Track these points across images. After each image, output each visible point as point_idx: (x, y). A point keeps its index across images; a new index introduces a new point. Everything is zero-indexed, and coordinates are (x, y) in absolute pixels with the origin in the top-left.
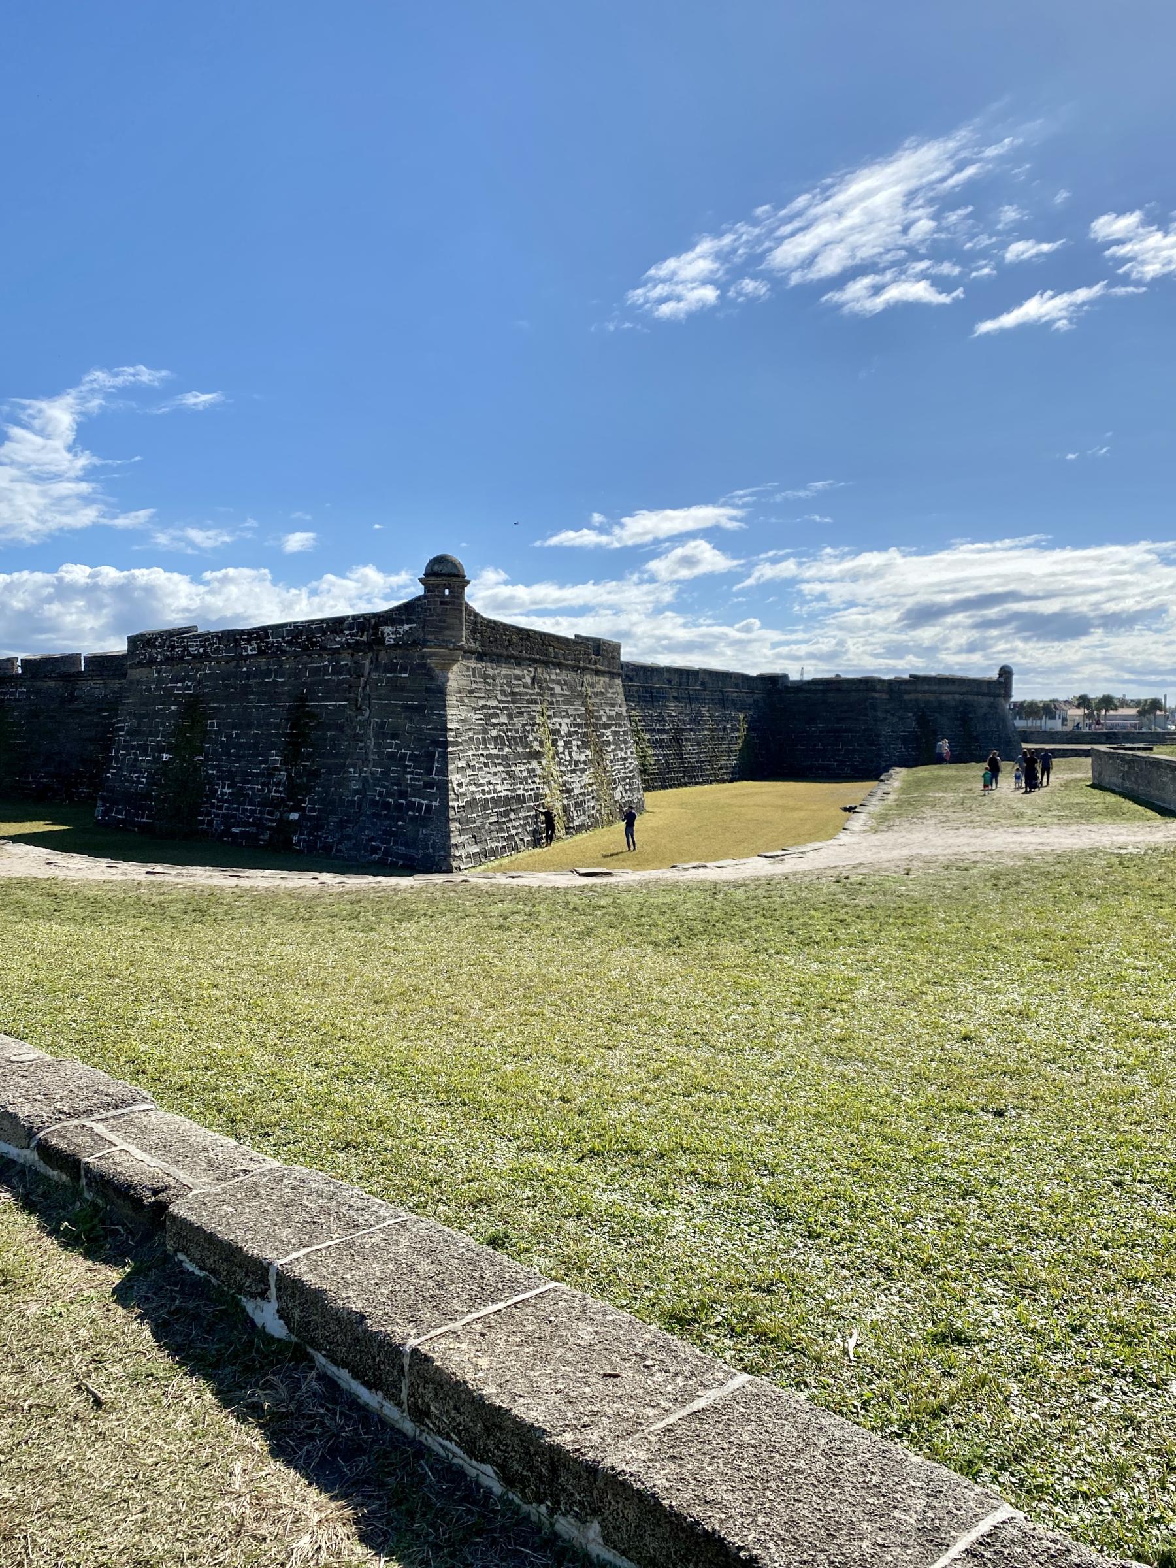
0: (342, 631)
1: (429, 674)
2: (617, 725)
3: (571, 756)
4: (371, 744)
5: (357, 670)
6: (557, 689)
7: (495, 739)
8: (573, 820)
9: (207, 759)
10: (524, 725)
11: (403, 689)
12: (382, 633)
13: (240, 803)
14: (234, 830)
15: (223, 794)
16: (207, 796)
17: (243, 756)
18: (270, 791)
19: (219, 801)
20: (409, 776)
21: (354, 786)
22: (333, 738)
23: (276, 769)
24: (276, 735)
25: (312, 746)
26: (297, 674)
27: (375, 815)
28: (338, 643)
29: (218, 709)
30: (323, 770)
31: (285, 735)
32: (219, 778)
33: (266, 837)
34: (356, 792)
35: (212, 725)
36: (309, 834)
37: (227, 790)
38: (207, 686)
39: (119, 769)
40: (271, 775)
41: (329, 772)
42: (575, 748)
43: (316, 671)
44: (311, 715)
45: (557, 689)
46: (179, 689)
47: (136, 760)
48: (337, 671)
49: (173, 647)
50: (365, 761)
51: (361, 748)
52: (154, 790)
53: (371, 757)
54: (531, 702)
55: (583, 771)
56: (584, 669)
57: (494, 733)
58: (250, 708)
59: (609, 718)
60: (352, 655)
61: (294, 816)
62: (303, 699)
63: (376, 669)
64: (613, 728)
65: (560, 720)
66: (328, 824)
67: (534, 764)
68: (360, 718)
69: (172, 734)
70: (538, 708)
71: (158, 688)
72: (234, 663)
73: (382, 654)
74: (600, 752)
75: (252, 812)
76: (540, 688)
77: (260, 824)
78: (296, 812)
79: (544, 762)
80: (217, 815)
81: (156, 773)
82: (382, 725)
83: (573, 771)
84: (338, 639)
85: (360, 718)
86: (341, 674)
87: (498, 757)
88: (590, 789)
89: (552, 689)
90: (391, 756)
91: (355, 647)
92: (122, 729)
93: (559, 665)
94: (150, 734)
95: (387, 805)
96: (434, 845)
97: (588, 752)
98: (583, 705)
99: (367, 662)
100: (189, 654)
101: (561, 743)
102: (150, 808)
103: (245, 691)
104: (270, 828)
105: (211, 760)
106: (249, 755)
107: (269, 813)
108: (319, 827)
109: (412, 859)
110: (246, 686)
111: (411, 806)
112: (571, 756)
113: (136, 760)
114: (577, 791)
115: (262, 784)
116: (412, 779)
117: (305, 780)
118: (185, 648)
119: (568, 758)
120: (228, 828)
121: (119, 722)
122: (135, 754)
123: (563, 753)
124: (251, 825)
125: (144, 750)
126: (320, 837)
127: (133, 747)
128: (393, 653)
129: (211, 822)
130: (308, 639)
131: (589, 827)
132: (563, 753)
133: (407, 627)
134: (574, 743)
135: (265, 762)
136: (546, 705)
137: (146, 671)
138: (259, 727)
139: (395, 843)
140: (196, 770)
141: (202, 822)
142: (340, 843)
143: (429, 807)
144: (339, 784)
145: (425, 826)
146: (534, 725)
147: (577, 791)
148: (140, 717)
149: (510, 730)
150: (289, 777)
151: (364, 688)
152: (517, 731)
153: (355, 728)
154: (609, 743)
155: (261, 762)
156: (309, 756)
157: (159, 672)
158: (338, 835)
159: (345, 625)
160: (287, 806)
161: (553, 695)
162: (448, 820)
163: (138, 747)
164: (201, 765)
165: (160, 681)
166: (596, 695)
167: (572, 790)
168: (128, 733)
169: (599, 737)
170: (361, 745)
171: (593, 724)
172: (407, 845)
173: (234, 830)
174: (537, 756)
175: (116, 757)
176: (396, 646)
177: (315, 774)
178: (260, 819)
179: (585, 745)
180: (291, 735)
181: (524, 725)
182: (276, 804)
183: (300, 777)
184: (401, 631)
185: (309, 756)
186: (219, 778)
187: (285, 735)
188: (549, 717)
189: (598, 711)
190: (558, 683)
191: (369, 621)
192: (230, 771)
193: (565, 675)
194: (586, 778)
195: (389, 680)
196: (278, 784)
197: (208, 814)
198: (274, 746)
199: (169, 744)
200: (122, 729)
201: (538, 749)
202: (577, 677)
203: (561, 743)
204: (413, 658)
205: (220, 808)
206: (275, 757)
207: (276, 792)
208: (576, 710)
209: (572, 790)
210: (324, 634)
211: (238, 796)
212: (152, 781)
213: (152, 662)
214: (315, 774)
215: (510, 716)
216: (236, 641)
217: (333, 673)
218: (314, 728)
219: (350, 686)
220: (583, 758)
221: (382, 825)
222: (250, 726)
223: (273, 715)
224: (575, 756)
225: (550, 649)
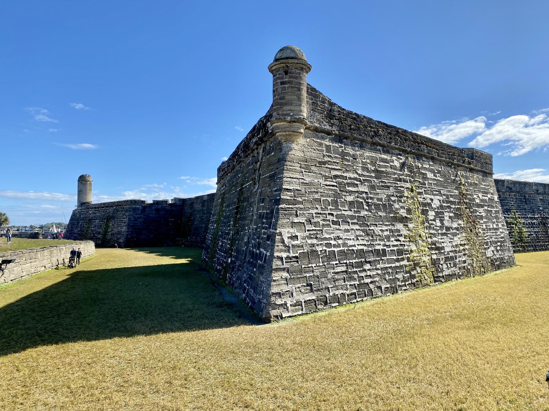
2: (488, 206)
3: (442, 221)
6: (430, 175)
7: (351, 203)
8: (442, 271)
10: (389, 196)
42: (447, 218)
45: (430, 175)
54: (400, 180)
55: (455, 235)
56: (459, 166)
57: (350, 198)
59: (482, 200)
64: (486, 208)
65: (432, 197)
67: (400, 226)
70: (408, 185)
74: (473, 221)
76: (410, 171)
79: (411, 226)
83: (443, 234)
87: (352, 217)
88: (462, 248)
89: (424, 174)
93: (433, 159)
97: (460, 222)
98: (457, 188)
101: (431, 214)
112: (443, 224)
114: (447, 249)
119: (439, 224)
123: (434, 220)
131: (461, 276)
132: (434, 220)
134: (446, 214)
136: (417, 184)
146: (401, 197)
147: (447, 249)
149: (371, 198)
152: (381, 200)
154: (481, 217)
161: (424, 177)
166: (470, 184)
167: (443, 248)
169: (471, 212)
171: (466, 203)
174: (404, 220)
179: (458, 216)
181: (389, 196)
188: (420, 193)
189: (472, 195)
190: (432, 171)
193: (436, 167)
194: (457, 240)
201: (405, 215)
202: (451, 171)
203: (431, 214)
208: (449, 191)
209: (443, 248)
215: (373, 187)
220: (455, 225)
224: (446, 224)
225: (423, 147)
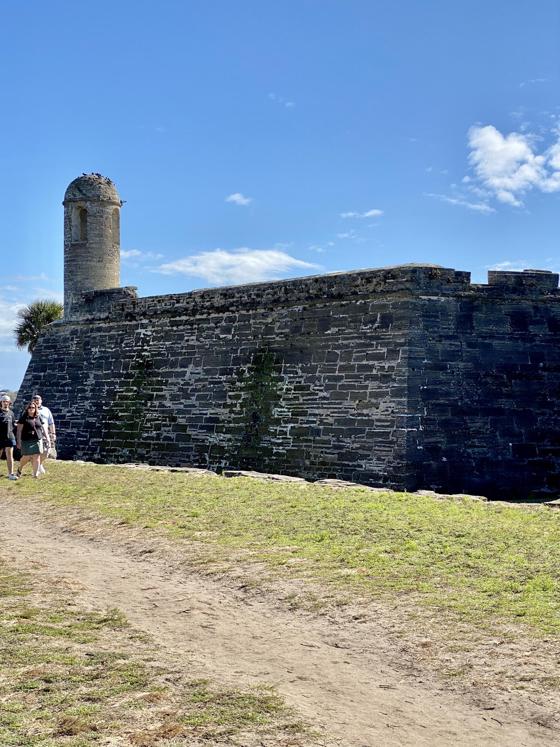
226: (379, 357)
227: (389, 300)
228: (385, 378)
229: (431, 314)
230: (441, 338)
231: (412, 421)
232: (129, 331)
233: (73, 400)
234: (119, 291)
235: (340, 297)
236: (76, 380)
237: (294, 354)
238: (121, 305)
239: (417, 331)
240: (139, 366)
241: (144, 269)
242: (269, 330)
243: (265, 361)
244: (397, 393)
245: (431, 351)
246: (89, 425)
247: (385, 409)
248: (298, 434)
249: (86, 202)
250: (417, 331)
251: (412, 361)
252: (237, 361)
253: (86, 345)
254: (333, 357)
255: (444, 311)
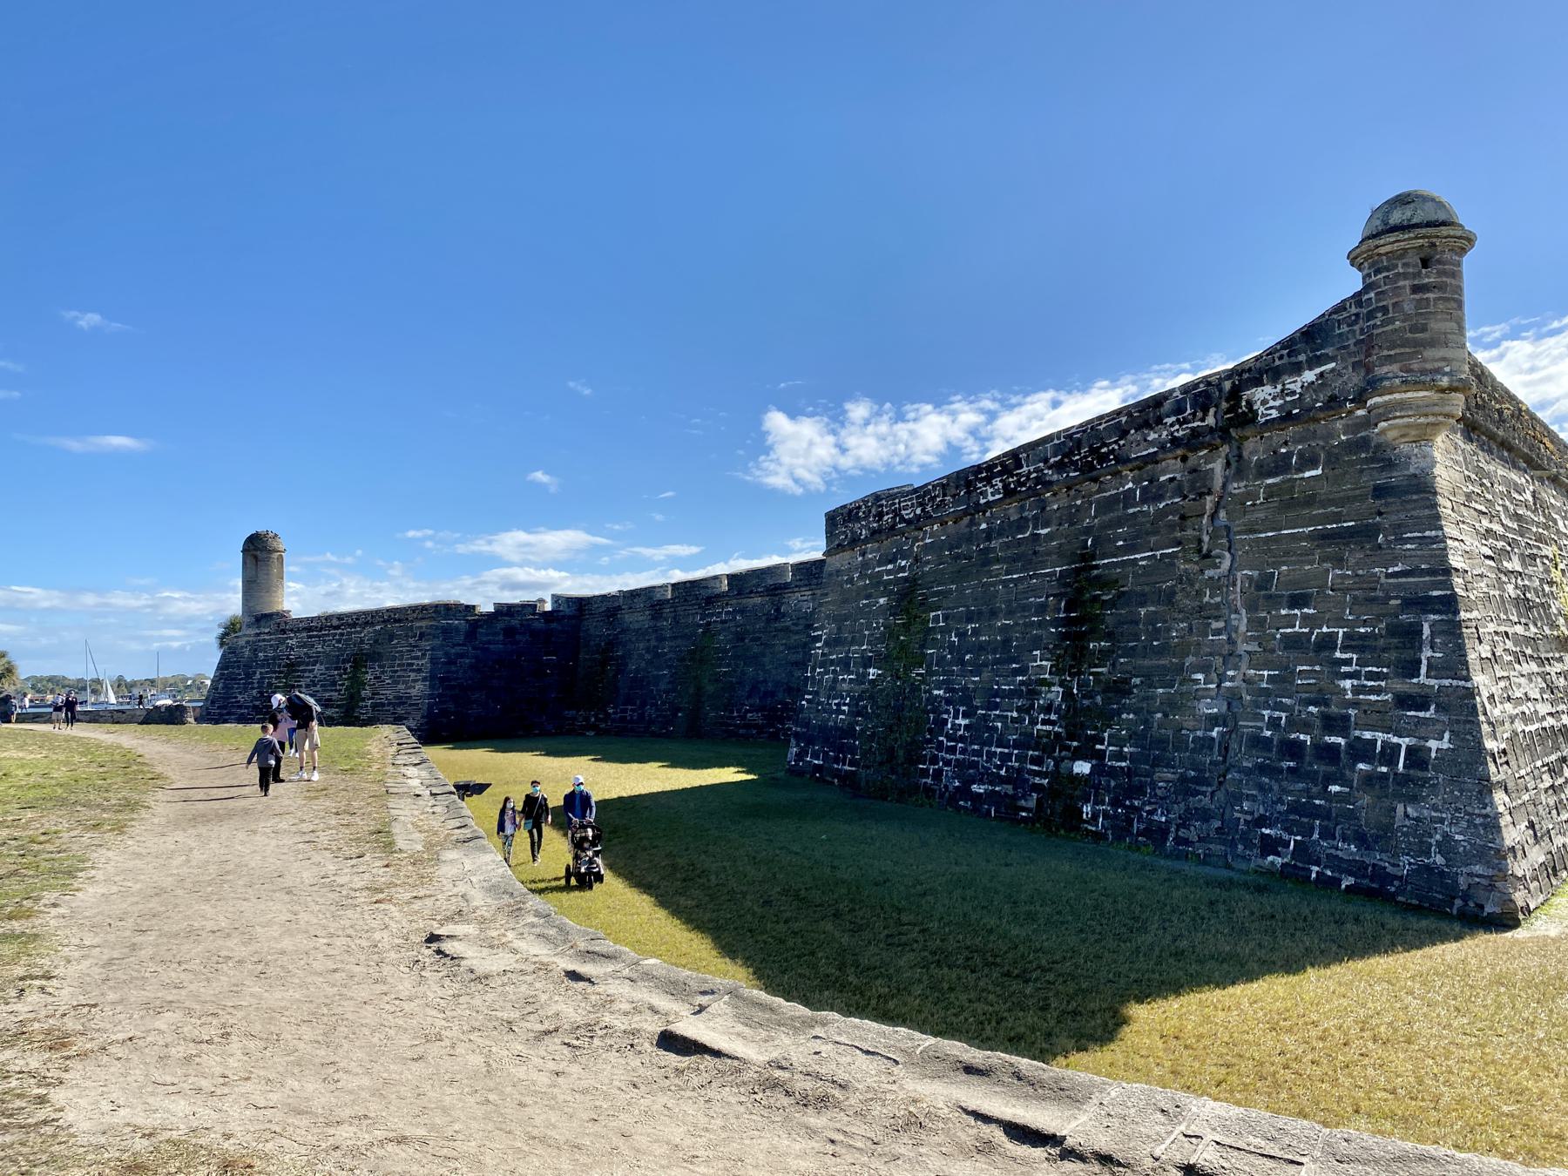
0: (1159, 421)
1: (1384, 459)
4: (1241, 621)
5: (1198, 484)
9: (930, 673)
11: (1310, 501)
12: (1250, 404)
13: (983, 744)
14: (975, 788)
15: (956, 727)
16: (931, 731)
17: (985, 665)
18: (1034, 722)
19: (949, 738)
20: (1347, 684)
21: (1209, 708)
22: (1152, 619)
23: (1043, 682)
24: (1040, 624)
25: (1109, 636)
26: (1072, 516)
27: (1262, 769)
28: (1152, 444)
29: (944, 594)
30: (1136, 681)
31: (1056, 622)
32: (948, 702)
33: (1032, 803)
34: (1214, 721)
35: (936, 619)
36: (1115, 803)
37: (962, 722)
38: (928, 562)
39: (816, 694)
40: (1033, 694)
41: (1149, 683)
43: (1107, 505)
44: (1103, 583)
46: (889, 572)
47: (835, 680)
48: (1150, 496)
49: (880, 515)
50: (1231, 657)
51: (1218, 632)
52: (857, 723)
53: (1243, 647)
58: (994, 584)
60: (1184, 459)
61: (1083, 768)
62: (1087, 557)
63: (1240, 474)
66: (1154, 786)
68: (1209, 573)
69: (881, 640)
71: (862, 576)
72: (966, 520)
73: (1249, 445)
75: (1005, 758)
77: (1017, 778)
78: (1085, 758)
80: (947, 763)
81: (861, 698)
82: (1264, 583)
84: (1152, 436)
85: (1209, 573)
86: (1160, 498)
90: (1293, 642)
91: (1194, 441)
92: (818, 639)
94: (852, 643)
95: (1293, 749)
96: (1447, 846)
99: (1218, 466)
100: (903, 520)
102: (853, 750)
103: (986, 559)
104: (1037, 788)
105: (937, 673)
106: (996, 662)
107: (1034, 761)
108: (1138, 791)
109: (1381, 876)
110: (987, 550)
111: (1362, 751)
113: (835, 680)
115: (1019, 710)
116: (1357, 690)
117: (1099, 699)
118: (897, 513)
120: (967, 783)
121: (816, 629)
122: (834, 672)
124: (1003, 781)
125: (845, 664)
126: (1138, 810)
127: (832, 662)
128: (1276, 436)
129: (938, 773)
130: (1093, 451)
133: (1309, 376)
135: (1022, 671)
137: (847, 555)
138: (1010, 614)
139: (1327, 834)
140: (915, 689)
141: (925, 773)
142: (1184, 824)
143: (1417, 757)
144: (1171, 705)
145: (1414, 799)
148: (839, 620)
150: (1068, 695)
151: (1213, 516)
153: (1200, 594)
155: (1016, 672)
156: (1104, 655)
157: (863, 554)
158: (1179, 809)
159: (1167, 405)
160: (1068, 748)
162: (1485, 787)
163: (839, 662)
164: (922, 682)
165: (865, 565)
168: (827, 644)
170: (1216, 625)
172: (1361, 840)
173: (975, 788)
175: (813, 677)
176: (1287, 418)
177: (1119, 689)
178: (1019, 771)
180: (1068, 622)
182: (1047, 745)
183: (1090, 695)
184: (1297, 387)
185: (1104, 655)
186: (948, 702)
187: (1056, 622)
191: (1219, 387)
192: (965, 689)
195: (1271, 492)
196: (1048, 709)
197: (934, 760)
198: (1036, 643)
199: (878, 653)
200: (818, 639)
204: (1331, 435)
205: (952, 750)
206: (1041, 663)
207: (1044, 722)
210: (1124, 434)
211: (980, 731)
212: (857, 711)
213: (855, 541)
214: (1119, 689)
216: (969, 484)
217: (1144, 501)
218: (1112, 604)
219: (1183, 518)
221: (1284, 791)
222: (994, 614)
223: (1034, 591)
226: (417, 658)
227: (423, 624)
228: (419, 671)
229: (447, 631)
230: (455, 645)
231: (431, 696)
232: (282, 642)
233: (245, 690)
234: (277, 614)
235: (399, 621)
236: (249, 676)
237: (374, 657)
238: (278, 623)
239: (437, 642)
240: (287, 665)
241: (299, 598)
242: (362, 642)
243: (360, 660)
244: (424, 679)
245: (446, 654)
246: (255, 707)
247: (418, 689)
248: (374, 706)
249: (258, 551)
250: (437, 642)
251: (433, 660)
252: (344, 661)
253: (255, 651)
254: (395, 658)
255: (457, 629)
